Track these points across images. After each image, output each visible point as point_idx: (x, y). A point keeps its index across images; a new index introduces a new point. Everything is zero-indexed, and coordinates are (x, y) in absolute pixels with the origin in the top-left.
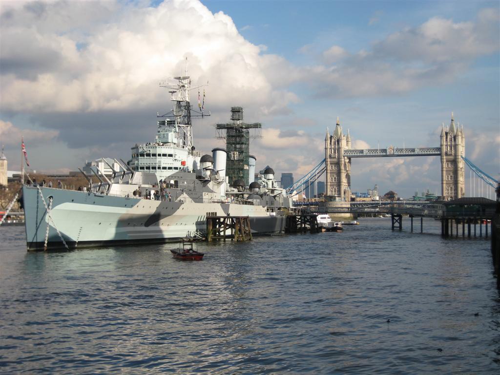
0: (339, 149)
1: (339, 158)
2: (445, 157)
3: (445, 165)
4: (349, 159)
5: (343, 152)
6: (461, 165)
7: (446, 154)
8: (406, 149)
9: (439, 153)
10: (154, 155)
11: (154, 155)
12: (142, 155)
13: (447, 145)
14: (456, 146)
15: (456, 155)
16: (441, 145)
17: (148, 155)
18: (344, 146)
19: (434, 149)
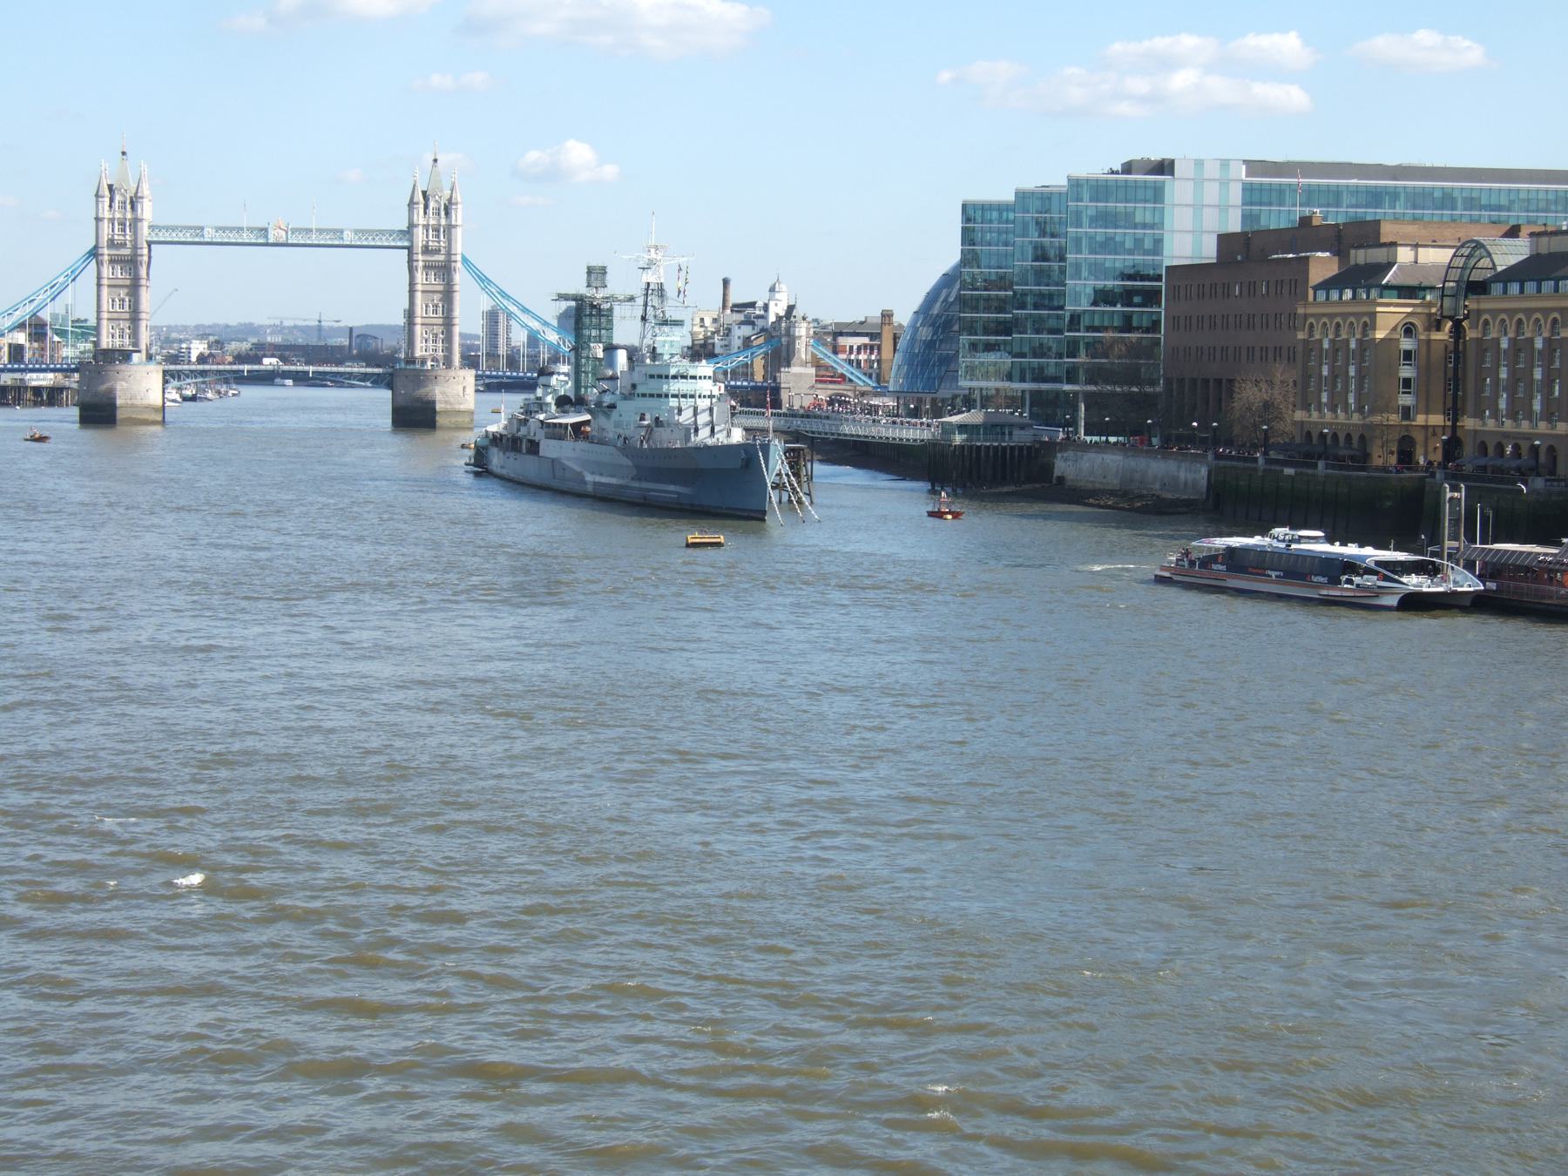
0: (136, 221)
1: (135, 247)
2: (420, 257)
3: (420, 276)
4: (149, 244)
5: (145, 233)
6: (460, 277)
7: (426, 250)
8: (320, 231)
9: (406, 244)
10: (694, 377)
11: (694, 377)
12: (675, 377)
13: (426, 227)
14: (450, 228)
15: (449, 254)
16: (412, 226)
17: (684, 377)
18: (147, 211)
19: (391, 233)
